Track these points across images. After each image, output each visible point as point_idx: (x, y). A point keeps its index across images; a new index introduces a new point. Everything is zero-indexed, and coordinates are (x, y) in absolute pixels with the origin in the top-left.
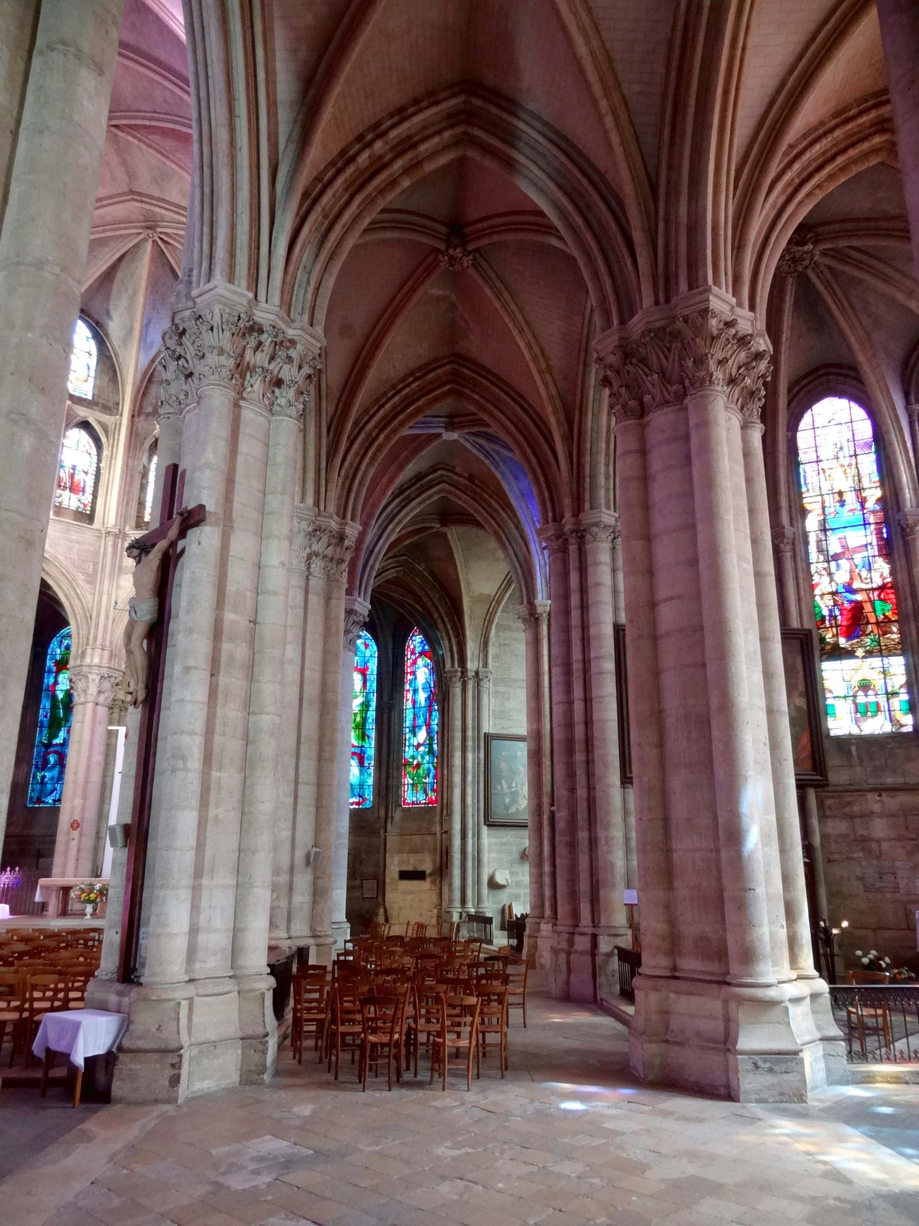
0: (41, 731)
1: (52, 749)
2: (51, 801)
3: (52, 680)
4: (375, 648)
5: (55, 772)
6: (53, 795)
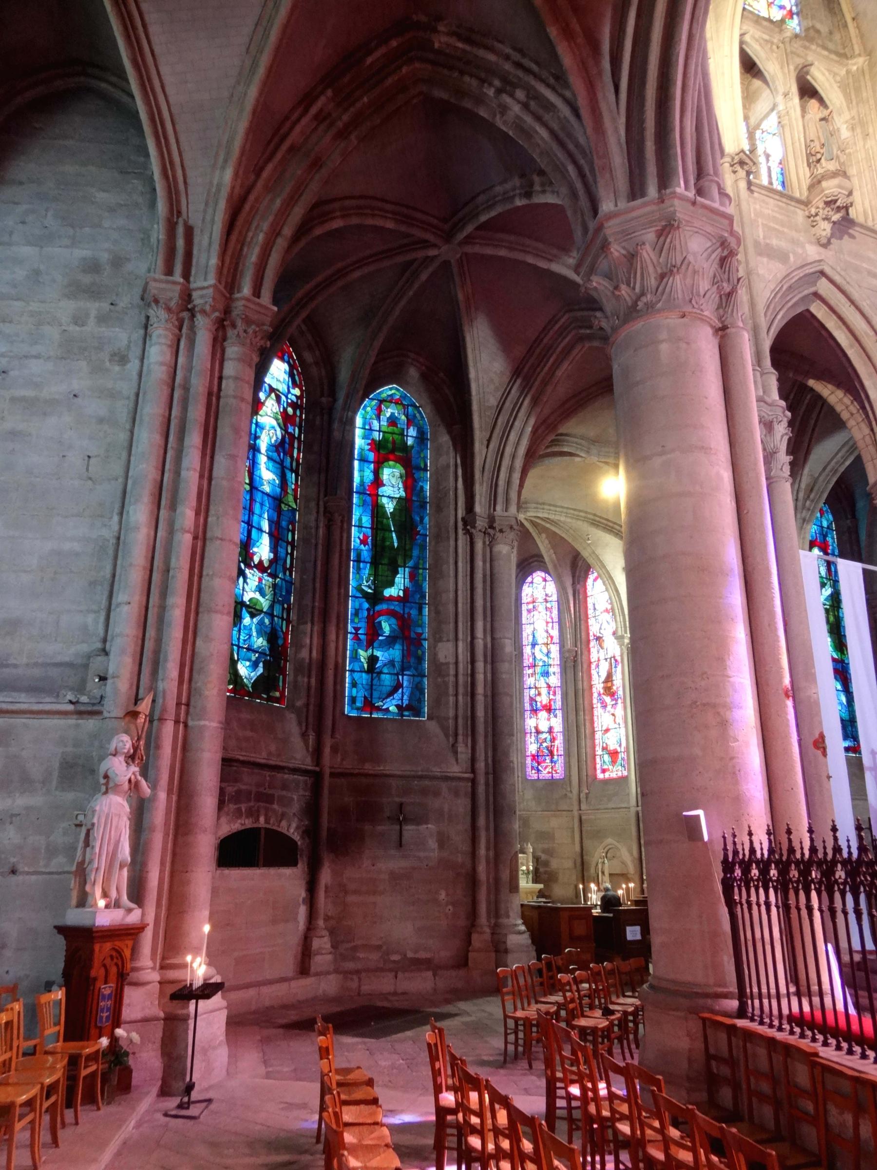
0: (358, 570)
1: (384, 606)
2: (392, 709)
3: (369, 476)
4: (831, 517)
5: (396, 653)
6: (397, 696)
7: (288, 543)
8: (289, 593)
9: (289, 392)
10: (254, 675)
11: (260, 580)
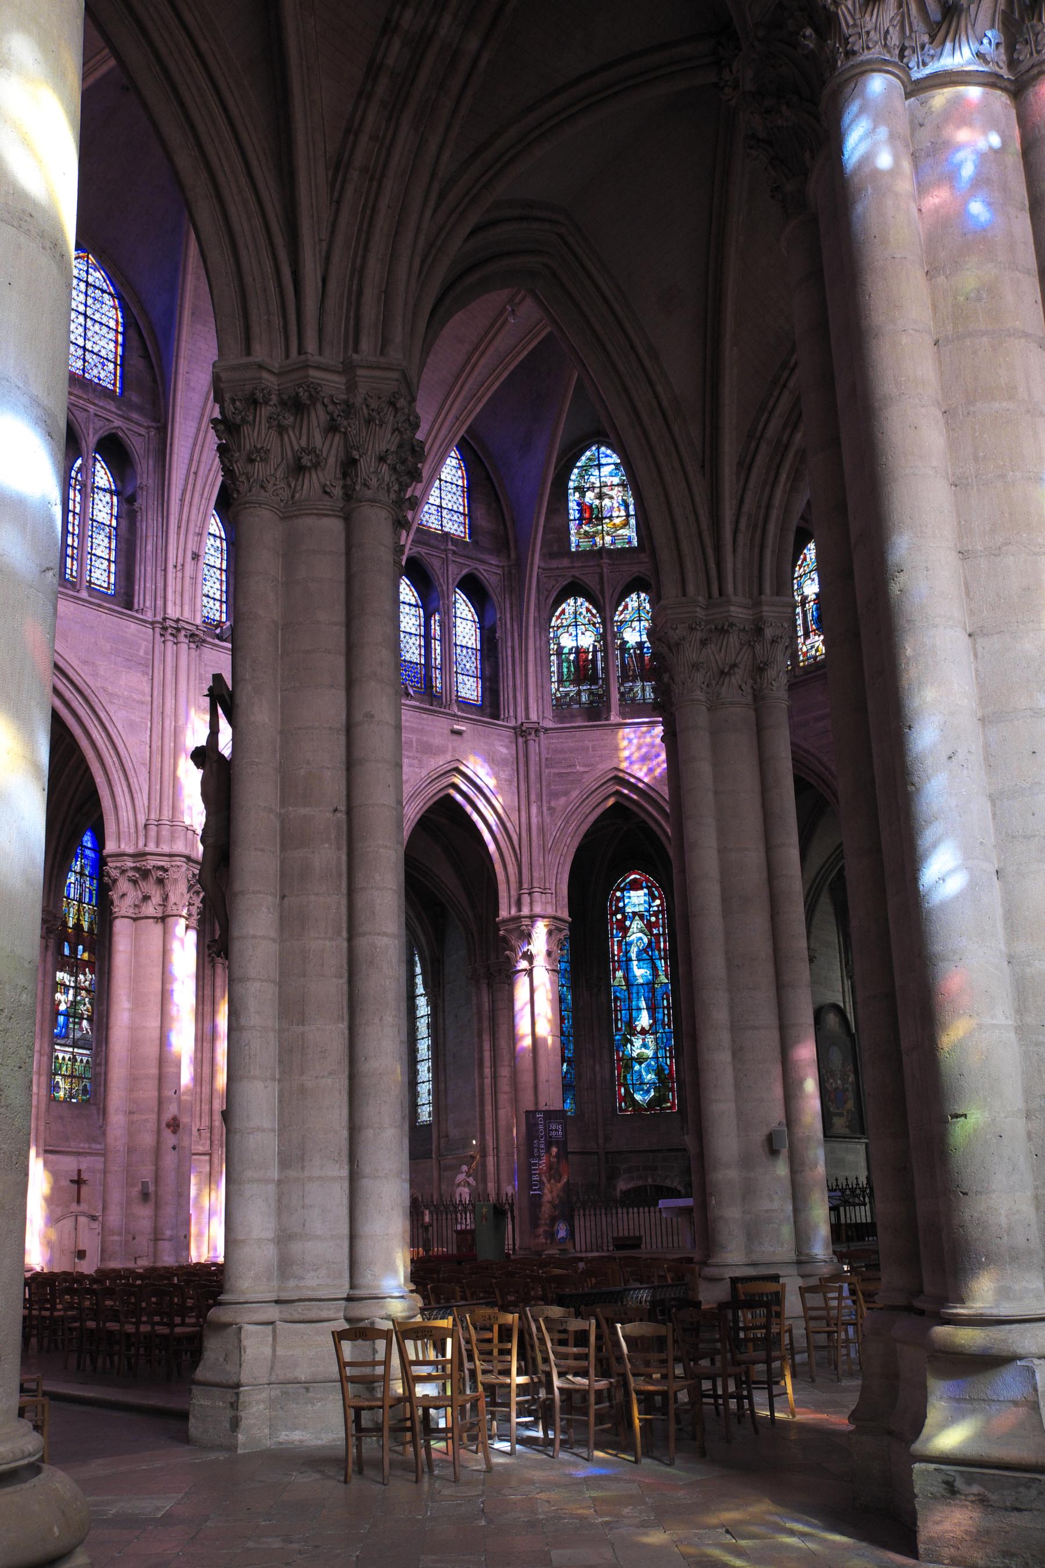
7: (664, 1008)
8: (669, 1040)
9: (650, 906)
10: (648, 1098)
11: (644, 1040)
